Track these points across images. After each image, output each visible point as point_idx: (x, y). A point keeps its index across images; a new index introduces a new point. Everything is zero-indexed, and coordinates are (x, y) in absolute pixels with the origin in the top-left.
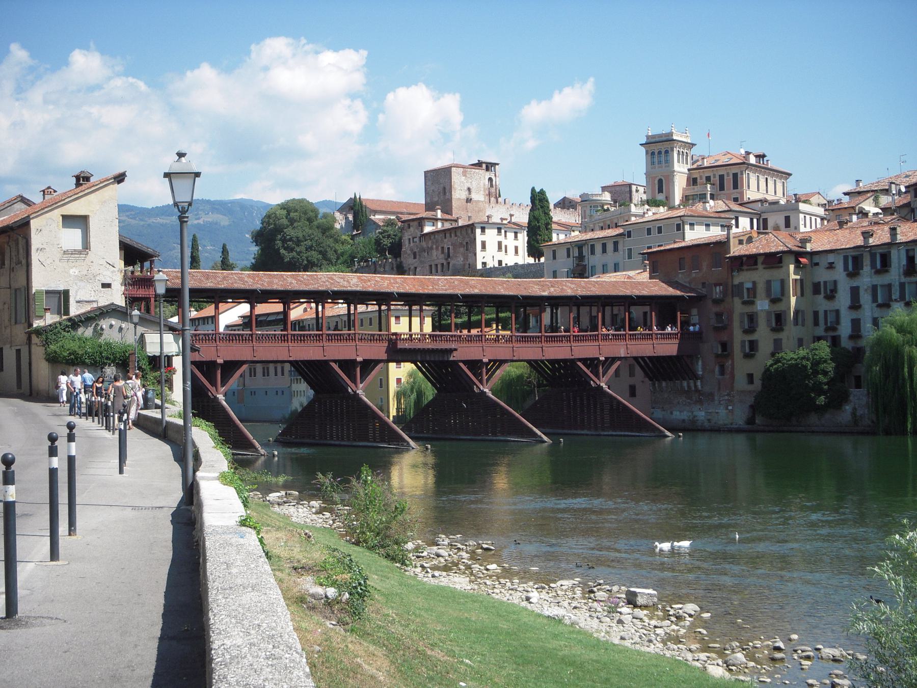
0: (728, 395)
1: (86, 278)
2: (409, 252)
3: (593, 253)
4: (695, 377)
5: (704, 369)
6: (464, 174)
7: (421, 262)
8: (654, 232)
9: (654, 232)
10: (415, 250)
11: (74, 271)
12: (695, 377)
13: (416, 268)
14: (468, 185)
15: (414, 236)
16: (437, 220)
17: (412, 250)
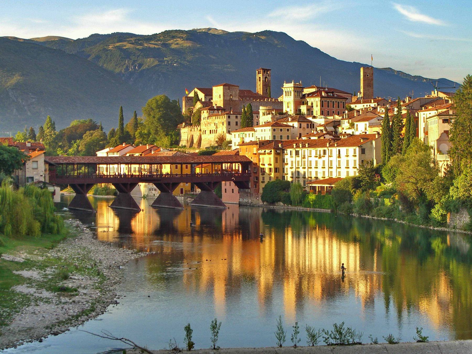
0: (257, 194)
1: (37, 174)
2: (203, 123)
3: (246, 137)
4: (249, 188)
5: (251, 186)
6: (229, 89)
7: (208, 129)
8: (263, 130)
9: (263, 130)
10: (206, 123)
11: (35, 173)
12: (249, 188)
13: (205, 131)
14: (231, 93)
15: (205, 116)
16: (216, 109)
17: (204, 123)
